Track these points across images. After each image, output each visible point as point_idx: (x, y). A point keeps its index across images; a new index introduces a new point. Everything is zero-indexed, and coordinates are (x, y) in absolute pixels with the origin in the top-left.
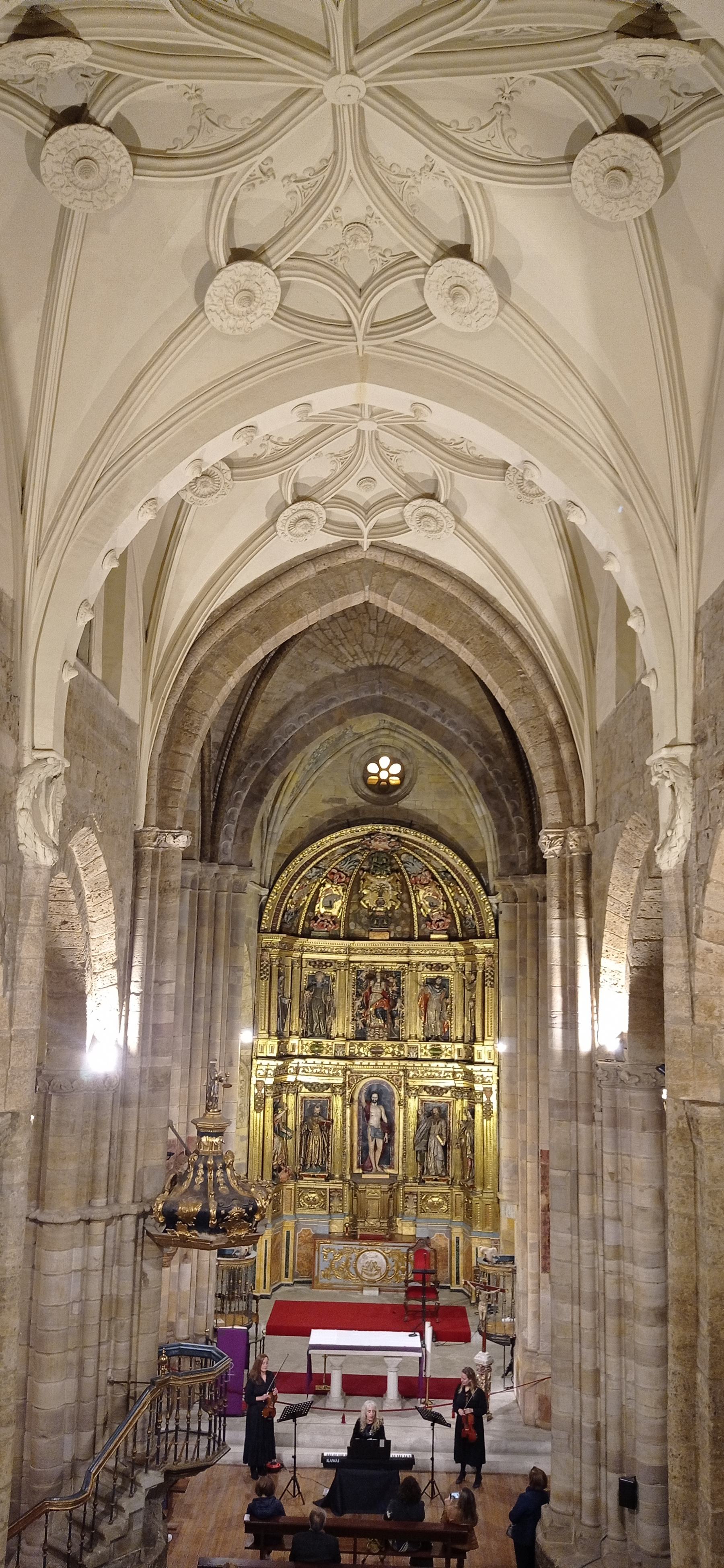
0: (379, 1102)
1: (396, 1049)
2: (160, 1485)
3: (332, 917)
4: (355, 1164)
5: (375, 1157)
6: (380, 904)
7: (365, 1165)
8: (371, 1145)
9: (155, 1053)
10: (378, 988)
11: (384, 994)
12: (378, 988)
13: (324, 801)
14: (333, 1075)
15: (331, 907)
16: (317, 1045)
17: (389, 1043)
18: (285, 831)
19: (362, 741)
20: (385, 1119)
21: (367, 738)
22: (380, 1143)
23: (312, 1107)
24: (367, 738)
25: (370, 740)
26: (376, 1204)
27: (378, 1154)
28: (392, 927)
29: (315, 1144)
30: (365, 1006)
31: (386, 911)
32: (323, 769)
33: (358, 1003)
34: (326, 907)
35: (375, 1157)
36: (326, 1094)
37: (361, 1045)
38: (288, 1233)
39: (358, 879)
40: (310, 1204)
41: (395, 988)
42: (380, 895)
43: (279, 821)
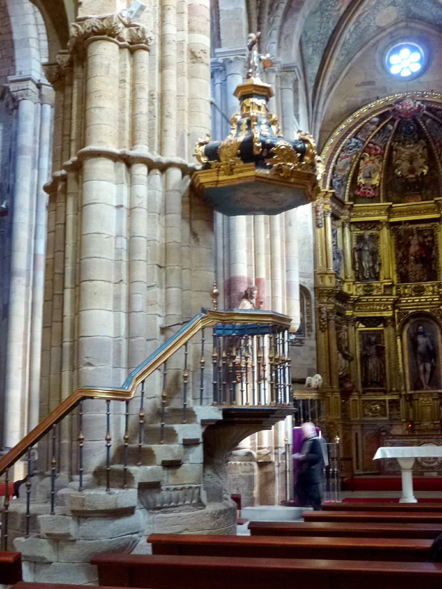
0: (423, 334)
1: (436, 287)
2: (218, 422)
3: (372, 186)
4: (408, 387)
5: (425, 379)
6: (412, 171)
7: (417, 385)
8: (421, 368)
9: (191, 30)
10: (414, 241)
11: (421, 245)
12: (414, 241)
13: (357, 86)
14: (384, 310)
15: (369, 177)
16: (369, 286)
17: (429, 283)
18: (327, 112)
19: (384, 34)
20: (431, 347)
21: (388, 31)
22: (428, 366)
23: (369, 339)
24: (388, 31)
25: (391, 33)
26: (428, 410)
27: (428, 376)
28: (423, 192)
29: (372, 364)
30: (405, 257)
31: (417, 177)
32: (353, 61)
33: (400, 255)
34: (366, 178)
35: (425, 379)
36: (380, 327)
37: (405, 287)
38: (357, 434)
39: (391, 149)
40: (373, 412)
41: (430, 239)
42: (411, 162)
43: (322, 102)
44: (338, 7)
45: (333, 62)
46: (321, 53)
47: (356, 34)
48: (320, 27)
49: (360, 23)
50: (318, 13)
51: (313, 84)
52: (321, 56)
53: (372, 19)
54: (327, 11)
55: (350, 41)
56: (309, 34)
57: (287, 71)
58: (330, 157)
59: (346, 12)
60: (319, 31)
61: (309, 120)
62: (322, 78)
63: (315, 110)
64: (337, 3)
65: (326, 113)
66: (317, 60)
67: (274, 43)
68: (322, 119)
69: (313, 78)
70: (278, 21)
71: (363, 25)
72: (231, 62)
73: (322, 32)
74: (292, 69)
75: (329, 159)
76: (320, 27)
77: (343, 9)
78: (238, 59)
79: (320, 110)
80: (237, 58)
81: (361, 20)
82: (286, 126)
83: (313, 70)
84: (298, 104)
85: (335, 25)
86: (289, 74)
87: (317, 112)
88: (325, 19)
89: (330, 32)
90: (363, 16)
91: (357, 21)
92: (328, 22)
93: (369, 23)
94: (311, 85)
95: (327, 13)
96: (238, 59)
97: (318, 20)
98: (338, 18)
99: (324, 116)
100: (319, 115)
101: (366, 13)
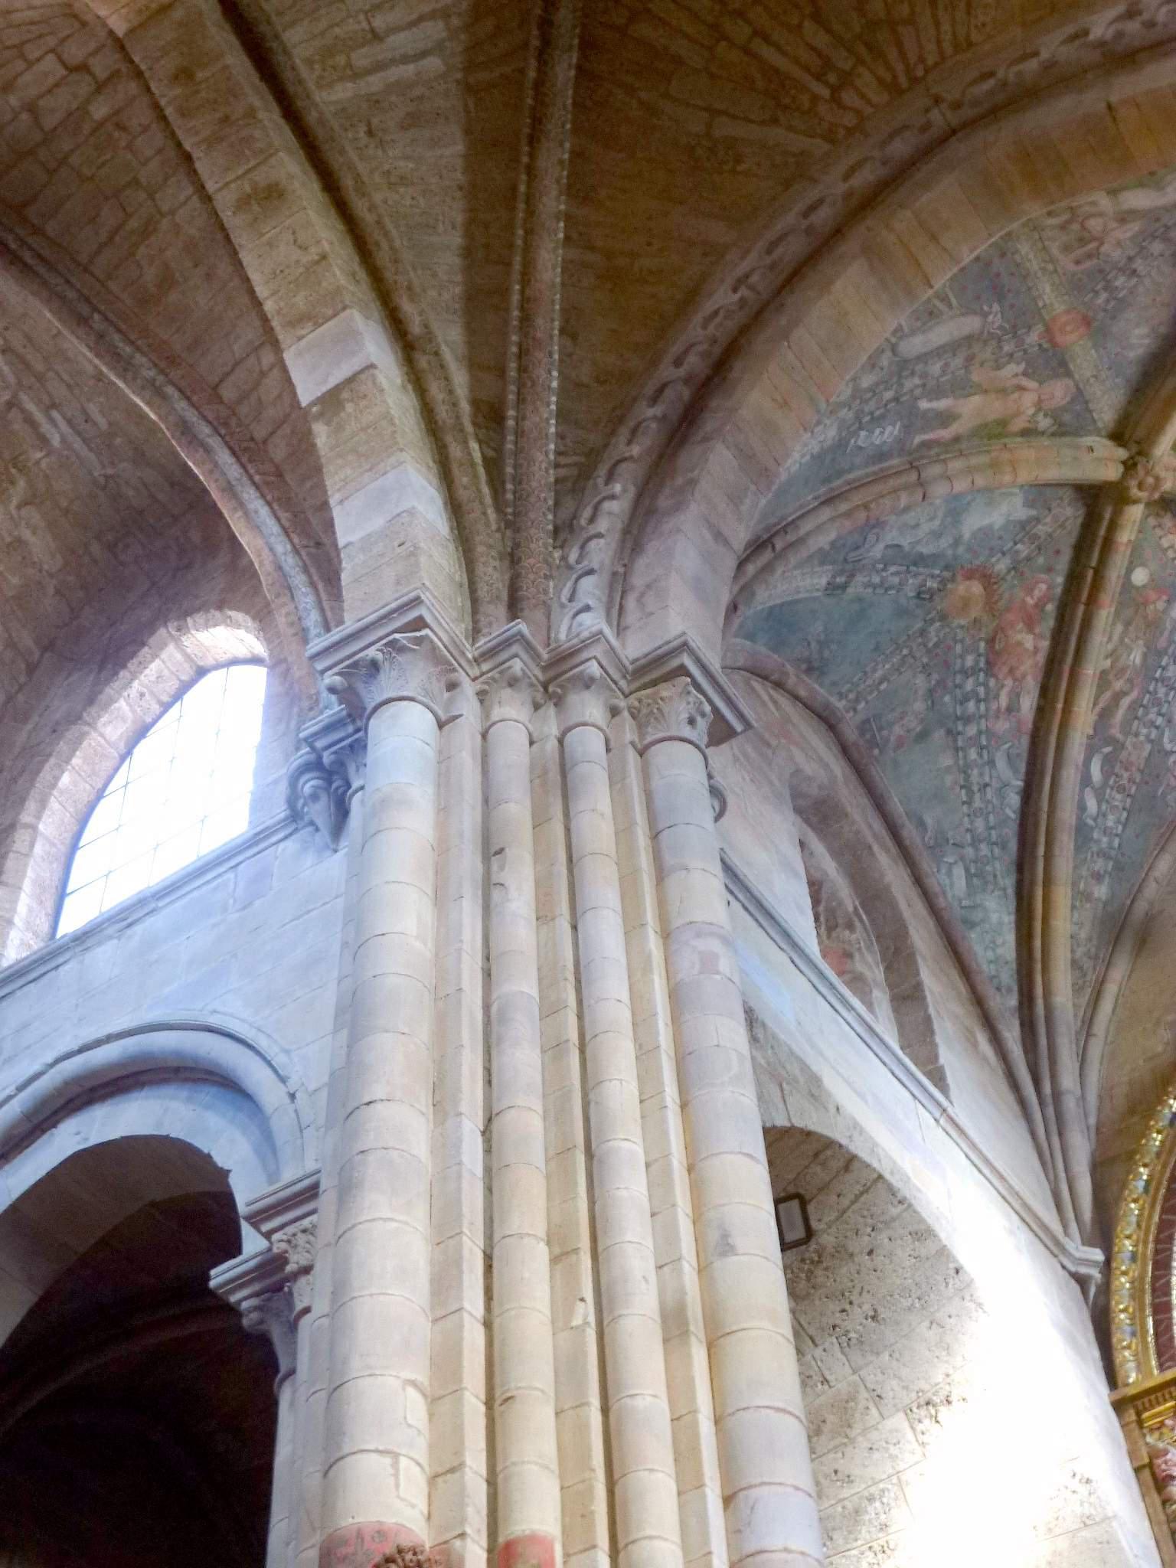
44: (1004, 700)
45: (1062, 896)
46: (1009, 882)
47: (1121, 789)
48: (967, 787)
49: (1119, 746)
50: (939, 734)
51: (1013, 1001)
52: (1011, 891)
53: (1159, 721)
54: (967, 720)
55: (1110, 821)
56: (929, 821)
57: (654, 683)
58: (1157, 1241)
59: (1042, 711)
60: (969, 803)
61: (1033, 1134)
62: (1038, 966)
63: (1047, 1089)
64: (992, 682)
65: (1100, 1097)
66: (998, 914)
67: (587, 608)
68: (1092, 1121)
69: (1008, 976)
70: (601, 552)
71: (1137, 752)
72: (374, 666)
73: (977, 803)
74: (675, 663)
75: (1157, 1252)
76: (967, 787)
77: (1028, 704)
78: (402, 650)
79: (1068, 1080)
80: (392, 644)
81: (1116, 732)
82: (669, 860)
83: (994, 942)
84: (932, 1032)
85: (1022, 767)
86: (665, 690)
87: (1057, 1095)
88: (973, 754)
89: (1014, 800)
90: (1120, 714)
91: (1100, 735)
92: (991, 763)
93: (1156, 743)
94: (1005, 1004)
95: (972, 730)
96: (402, 650)
97: (947, 761)
98: (1025, 742)
99: (1100, 1110)
100: (1070, 1103)
101: (1125, 702)
